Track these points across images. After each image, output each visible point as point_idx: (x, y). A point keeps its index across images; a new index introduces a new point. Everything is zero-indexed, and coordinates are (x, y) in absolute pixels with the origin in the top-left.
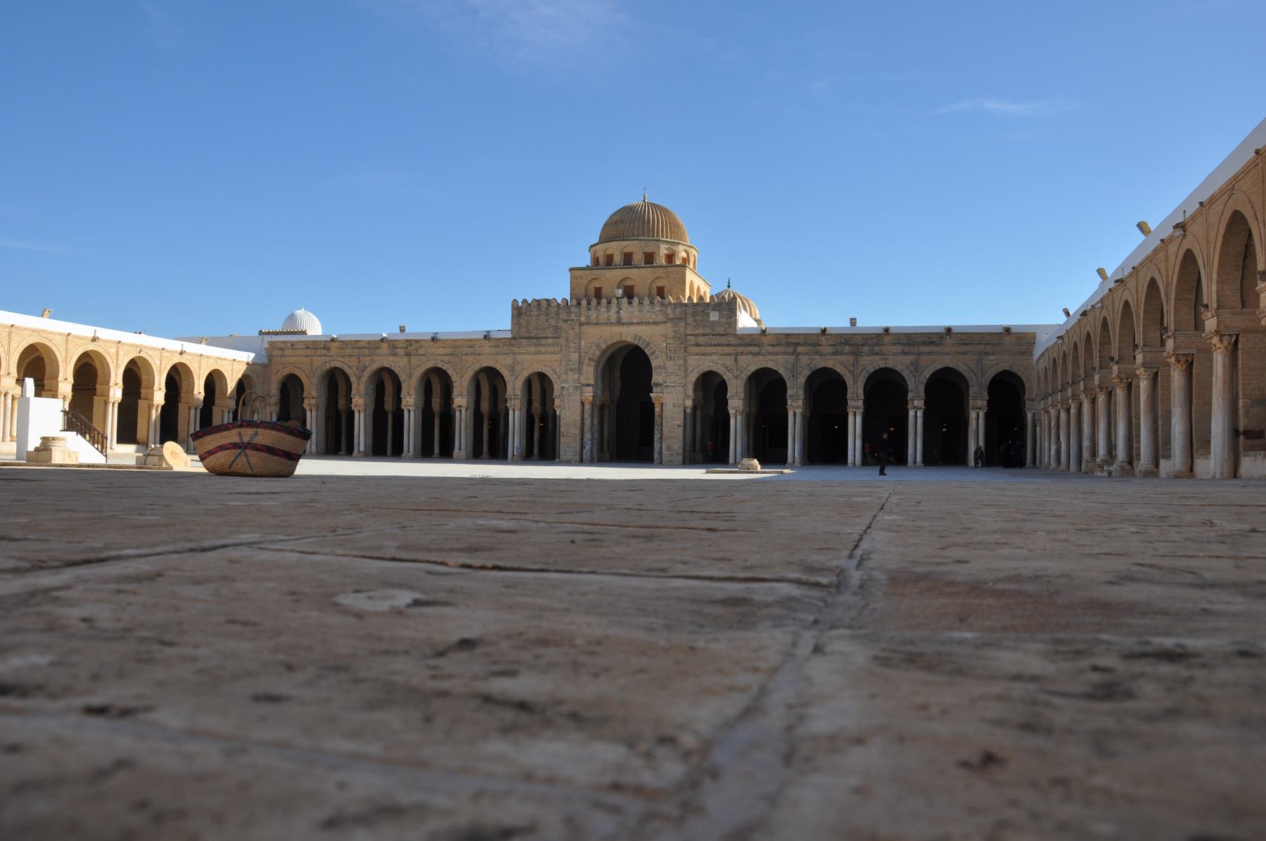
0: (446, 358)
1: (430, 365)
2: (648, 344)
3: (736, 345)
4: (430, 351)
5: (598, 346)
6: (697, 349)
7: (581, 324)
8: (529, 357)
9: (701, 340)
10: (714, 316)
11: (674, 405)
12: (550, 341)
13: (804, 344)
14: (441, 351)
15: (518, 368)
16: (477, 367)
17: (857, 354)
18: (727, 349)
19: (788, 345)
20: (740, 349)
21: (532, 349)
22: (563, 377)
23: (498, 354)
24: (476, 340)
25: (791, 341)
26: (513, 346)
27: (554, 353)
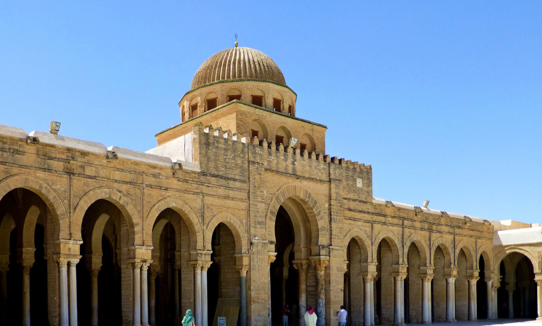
0: (124, 188)
1: (102, 194)
2: (316, 203)
3: (373, 214)
4: (103, 173)
5: (277, 198)
6: (349, 214)
7: (266, 170)
8: (217, 201)
9: (352, 205)
10: (359, 183)
11: (338, 270)
12: (238, 184)
13: (408, 219)
14: (117, 175)
15: (207, 214)
16: (162, 207)
17: (430, 230)
18: (368, 217)
19: (400, 218)
20: (375, 218)
21: (222, 191)
22: (252, 231)
23: (186, 191)
24: (161, 168)
25: (403, 216)
26: (202, 184)
27: (241, 200)
